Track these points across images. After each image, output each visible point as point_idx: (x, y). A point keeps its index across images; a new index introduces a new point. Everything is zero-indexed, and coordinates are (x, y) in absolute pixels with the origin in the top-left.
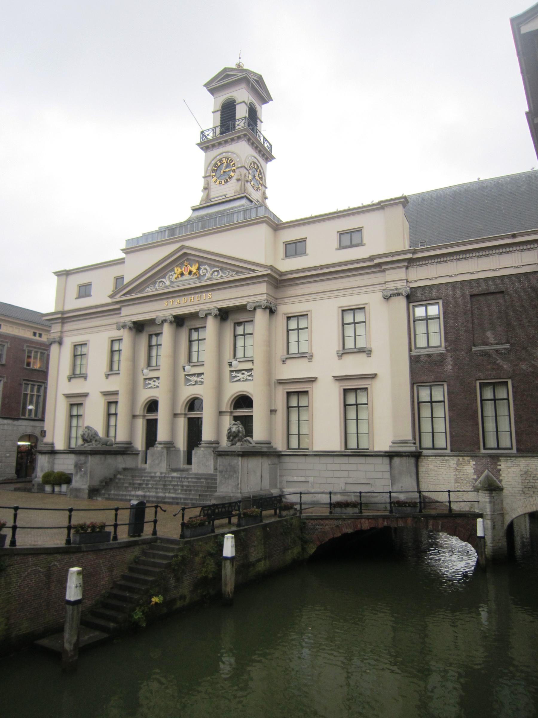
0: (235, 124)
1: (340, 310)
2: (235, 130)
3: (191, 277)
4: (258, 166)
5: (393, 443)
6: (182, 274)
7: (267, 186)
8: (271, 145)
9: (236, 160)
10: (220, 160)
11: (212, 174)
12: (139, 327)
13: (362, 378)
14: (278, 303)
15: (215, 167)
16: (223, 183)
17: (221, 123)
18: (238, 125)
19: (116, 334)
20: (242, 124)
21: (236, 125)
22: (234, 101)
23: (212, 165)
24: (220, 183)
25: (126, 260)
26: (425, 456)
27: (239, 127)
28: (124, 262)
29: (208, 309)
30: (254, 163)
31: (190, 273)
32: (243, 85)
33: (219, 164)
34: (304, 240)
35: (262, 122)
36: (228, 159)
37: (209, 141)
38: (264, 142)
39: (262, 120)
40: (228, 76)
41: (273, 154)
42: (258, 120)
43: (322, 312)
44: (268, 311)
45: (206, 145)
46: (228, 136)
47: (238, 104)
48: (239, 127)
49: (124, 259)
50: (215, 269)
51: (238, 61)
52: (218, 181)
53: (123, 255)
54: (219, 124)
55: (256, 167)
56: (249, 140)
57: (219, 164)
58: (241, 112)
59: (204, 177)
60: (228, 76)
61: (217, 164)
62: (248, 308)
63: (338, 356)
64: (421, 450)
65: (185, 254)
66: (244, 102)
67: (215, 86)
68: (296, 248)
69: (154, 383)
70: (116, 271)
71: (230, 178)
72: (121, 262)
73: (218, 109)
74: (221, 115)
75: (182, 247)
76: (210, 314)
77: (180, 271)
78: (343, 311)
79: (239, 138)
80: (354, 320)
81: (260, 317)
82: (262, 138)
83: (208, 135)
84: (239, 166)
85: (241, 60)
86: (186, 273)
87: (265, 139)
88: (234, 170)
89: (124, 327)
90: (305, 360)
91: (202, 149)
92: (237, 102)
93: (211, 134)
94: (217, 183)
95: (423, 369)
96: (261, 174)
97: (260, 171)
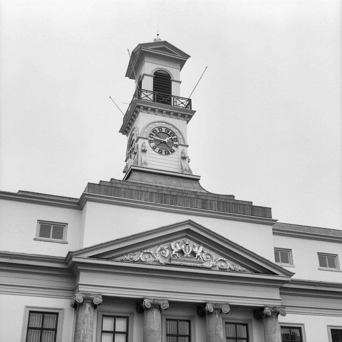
1: (330, 328)
3: (194, 259)
6: (181, 252)
11: (150, 138)
16: (164, 153)
24: (160, 152)
31: (193, 254)
33: (158, 132)
40: (163, 49)
50: (222, 258)
52: (157, 149)
57: (158, 132)
61: (156, 131)
65: (188, 230)
71: (171, 151)
73: (149, 74)
75: (190, 222)
77: (179, 248)
84: (182, 143)
86: (187, 253)
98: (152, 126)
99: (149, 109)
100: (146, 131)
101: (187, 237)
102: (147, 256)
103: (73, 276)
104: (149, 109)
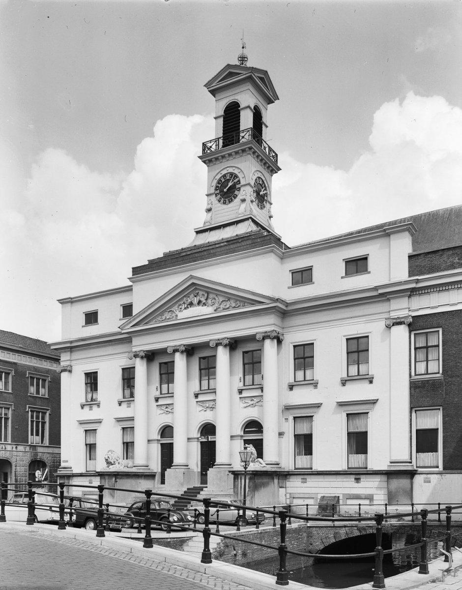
0: (239, 136)
2: (239, 142)
4: (263, 181)
5: (391, 463)
9: (240, 176)
10: (224, 176)
12: (150, 356)
13: (367, 403)
14: (284, 331)
15: (219, 183)
17: (224, 134)
18: (243, 137)
19: (125, 362)
20: (247, 137)
21: (241, 138)
23: (215, 182)
25: (134, 288)
26: (419, 474)
27: (243, 140)
28: (131, 290)
29: (219, 340)
33: (223, 180)
34: (310, 269)
35: (267, 127)
36: (232, 175)
37: (212, 153)
39: (268, 125)
42: (263, 126)
43: (329, 339)
44: (275, 341)
45: (208, 157)
46: (232, 149)
47: (242, 109)
48: (243, 140)
49: (132, 286)
53: (131, 284)
54: (222, 135)
55: (261, 183)
56: (254, 153)
58: (246, 121)
59: (207, 195)
61: (221, 181)
62: (257, 337)
63: (342, 383)
64: (417, 469)
65: (193, 284)
66: (249, 107)
68: (303, 276)
69: (166, 409)
70: (125, 299)
72: (128, 289)
74: (224, 121)
76: (220, 344)
78: (347, 340)
79: (243, 151)
80: (358, 348)
81: (269, 347)
82: (267, 149)
83: (211, 147)
84: (244, 183)
87: (270, 149)
88: (239, 188)
89: (136, 356)
90: (311, 388)
91: (204, 162)
93: (214, 147)
94: (222, 201)
95: (422, 393)
98: (218, 177)
99: (220, 158)
100: (213, 185)
101: (196, 289)
102: (170, 314)
104: (220, 158)
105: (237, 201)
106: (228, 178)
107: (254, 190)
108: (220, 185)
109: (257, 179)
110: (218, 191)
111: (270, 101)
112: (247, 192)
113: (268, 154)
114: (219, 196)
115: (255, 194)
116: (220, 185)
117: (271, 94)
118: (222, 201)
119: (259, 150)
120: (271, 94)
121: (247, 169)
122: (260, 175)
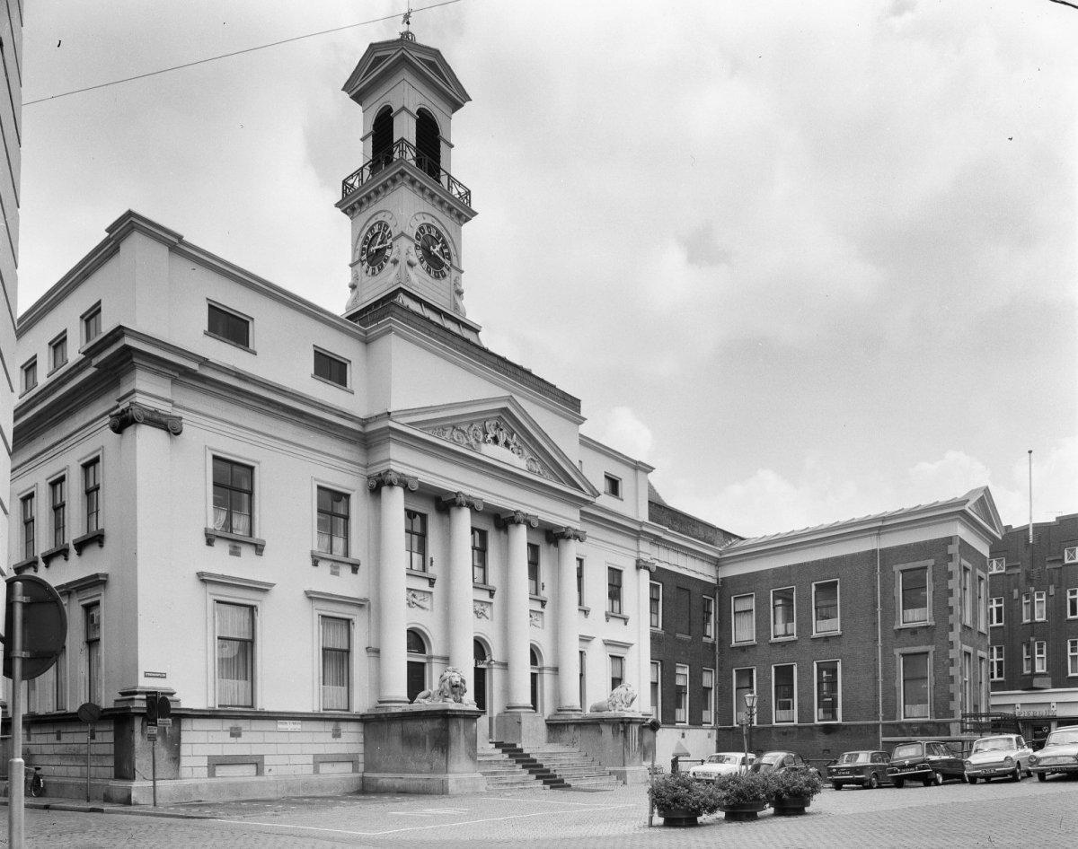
4: (438, 232)
7: (463, 268)
8: (468, 193)
22: (390, 110)
30: (429, 226)
32: (405, 75)
35: (452, 146)
38: (449, 187)
40: (379, 60)
41: (474, 207)
42: (442, 144)
51: (404, 28)
55: (434, 234)
60: (379, 60)
67: (362, 85)
85: (412, 28)
92: (395, 111)
96: (446, 247)
97: (443, 241)
103: (366, 467)
105: (389, 265)
106: (376, 231)
107: (416, 246)
108: (366, 246)
109: (425, 227)
110: (365, 257)
111: (456, 106)
112: (405, 250)
113: (446, 188)
114: (366, 264)
115: (420, 253)
116: (366, 246)
117: (455, 91)
118: (370, 273)
119: (430, 185)
120: (455, 91)
121: (405, 209)
122: (429, 220)
